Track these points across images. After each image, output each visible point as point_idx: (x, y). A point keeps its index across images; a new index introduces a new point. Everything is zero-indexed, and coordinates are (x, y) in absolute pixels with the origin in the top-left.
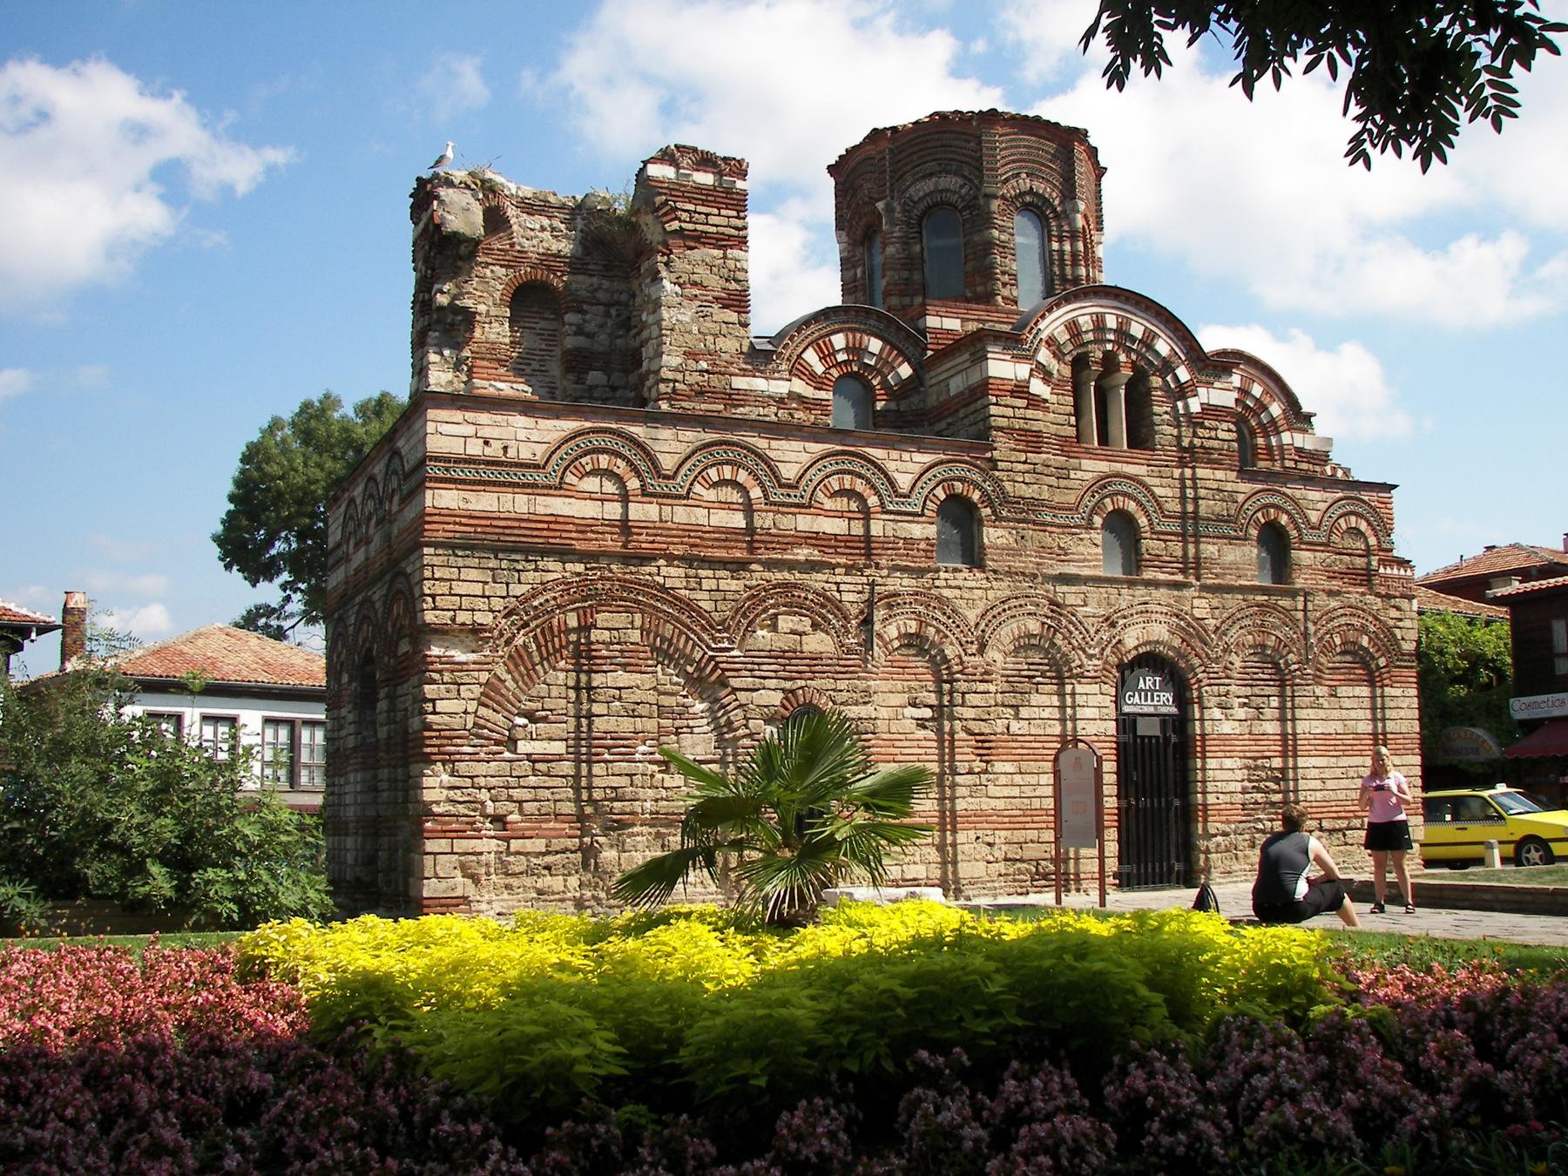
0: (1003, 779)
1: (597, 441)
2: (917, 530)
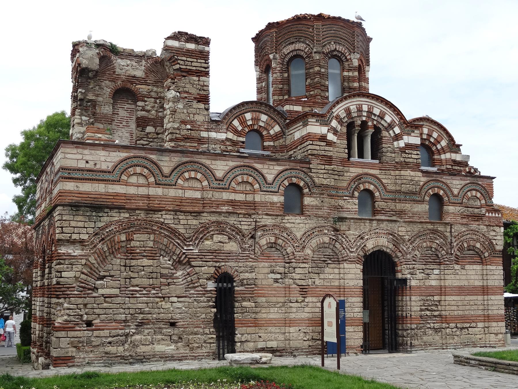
0: (310, 305)
1: (135, 161)
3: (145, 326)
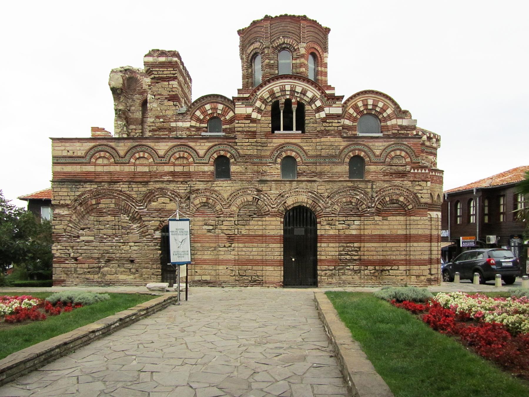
1: (100, 148)
2: (206, 168)
3: (111, 262)
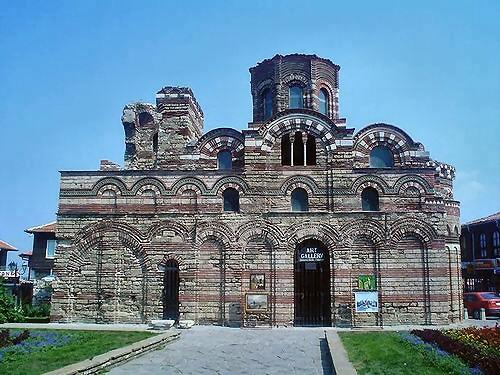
2: (214, 201)
